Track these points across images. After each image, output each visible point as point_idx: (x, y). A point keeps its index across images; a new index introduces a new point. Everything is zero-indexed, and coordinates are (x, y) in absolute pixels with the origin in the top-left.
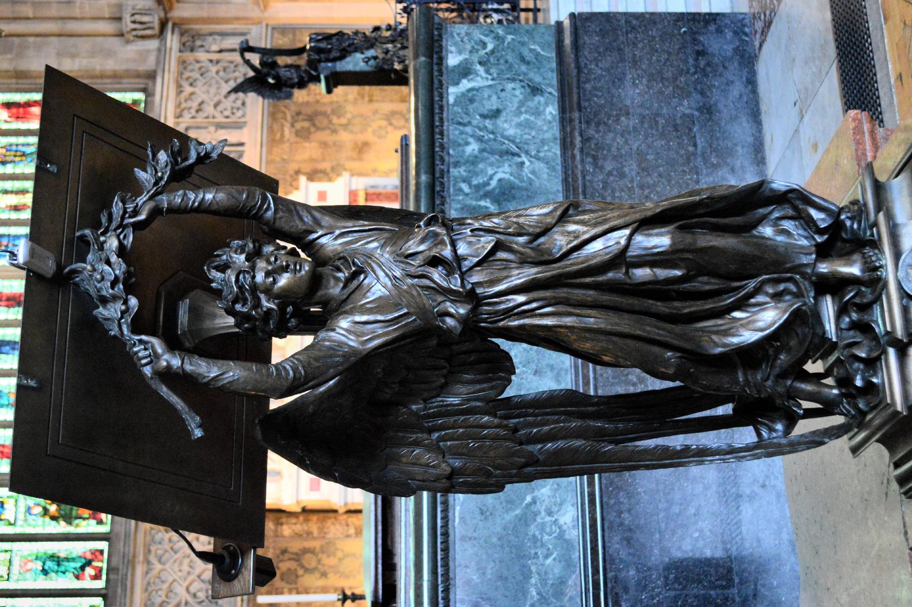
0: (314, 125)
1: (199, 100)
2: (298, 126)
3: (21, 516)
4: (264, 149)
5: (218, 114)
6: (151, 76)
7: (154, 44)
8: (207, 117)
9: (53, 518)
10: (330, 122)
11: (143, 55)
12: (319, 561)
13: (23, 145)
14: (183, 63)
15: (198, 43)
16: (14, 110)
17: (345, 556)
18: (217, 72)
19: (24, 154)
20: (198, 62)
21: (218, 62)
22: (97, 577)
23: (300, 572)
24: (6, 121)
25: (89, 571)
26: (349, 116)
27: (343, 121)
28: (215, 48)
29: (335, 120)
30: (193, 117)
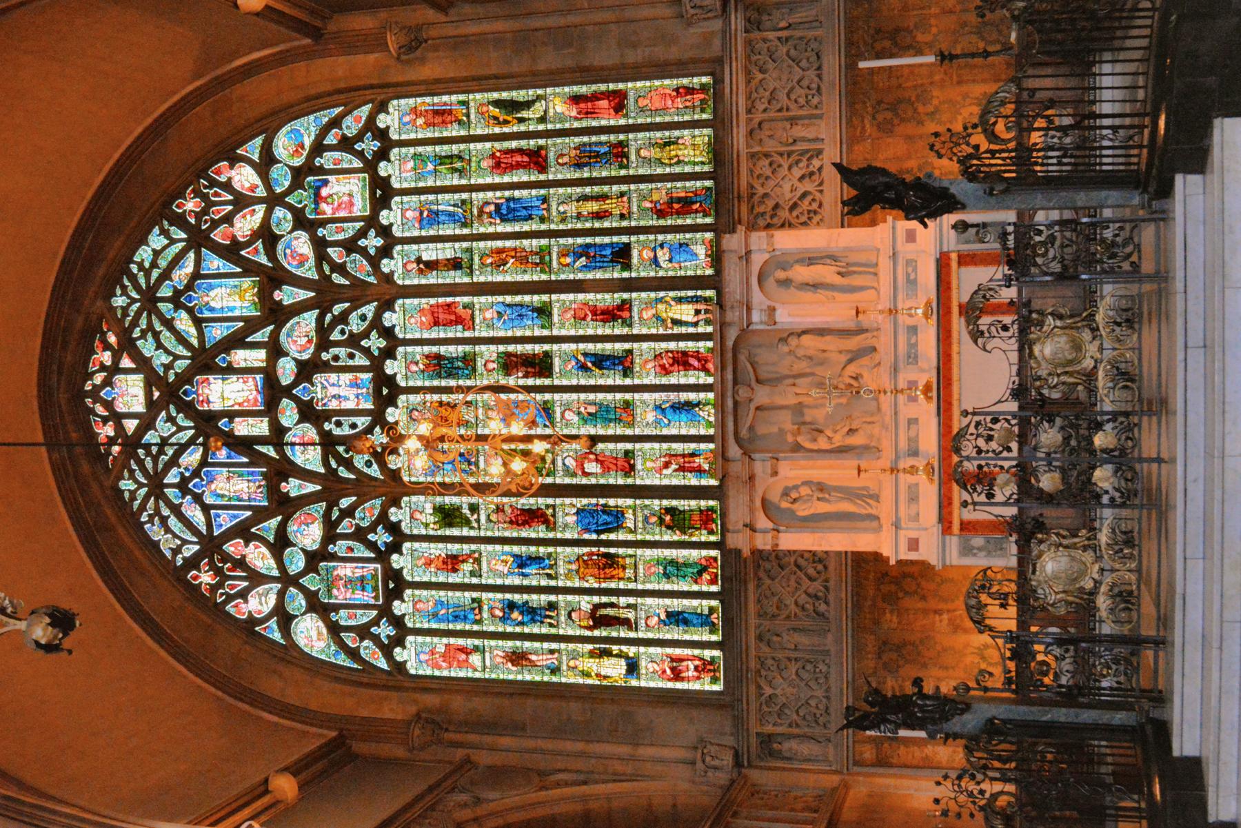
0: (897, 115)
1: (772, 88)
2: (880, 117)
3: (640, 525)
4: (844, 146)
5: (793, 106)
6: (719, 61)
7: (717, 25)
8: (780, 110)
9: (668, 527)
10: (915, 110)
11: (707, 38)
12: (918, 585)
13: (596, 144)
14: (749, 43)
15: (765, 17)
16: (582, 105)
17: (945, 650)
18: (788, 54)
19: (598, 155)
20: (765, 40)
21: (787, 39)
22: (713, 582)
23: (901, 595)
24: (576, 119)
25: (706, 576)
26: (935, 102)
27: (930, 109)
28: (783, 24)
29: (921, 109)
30: (765, 110)
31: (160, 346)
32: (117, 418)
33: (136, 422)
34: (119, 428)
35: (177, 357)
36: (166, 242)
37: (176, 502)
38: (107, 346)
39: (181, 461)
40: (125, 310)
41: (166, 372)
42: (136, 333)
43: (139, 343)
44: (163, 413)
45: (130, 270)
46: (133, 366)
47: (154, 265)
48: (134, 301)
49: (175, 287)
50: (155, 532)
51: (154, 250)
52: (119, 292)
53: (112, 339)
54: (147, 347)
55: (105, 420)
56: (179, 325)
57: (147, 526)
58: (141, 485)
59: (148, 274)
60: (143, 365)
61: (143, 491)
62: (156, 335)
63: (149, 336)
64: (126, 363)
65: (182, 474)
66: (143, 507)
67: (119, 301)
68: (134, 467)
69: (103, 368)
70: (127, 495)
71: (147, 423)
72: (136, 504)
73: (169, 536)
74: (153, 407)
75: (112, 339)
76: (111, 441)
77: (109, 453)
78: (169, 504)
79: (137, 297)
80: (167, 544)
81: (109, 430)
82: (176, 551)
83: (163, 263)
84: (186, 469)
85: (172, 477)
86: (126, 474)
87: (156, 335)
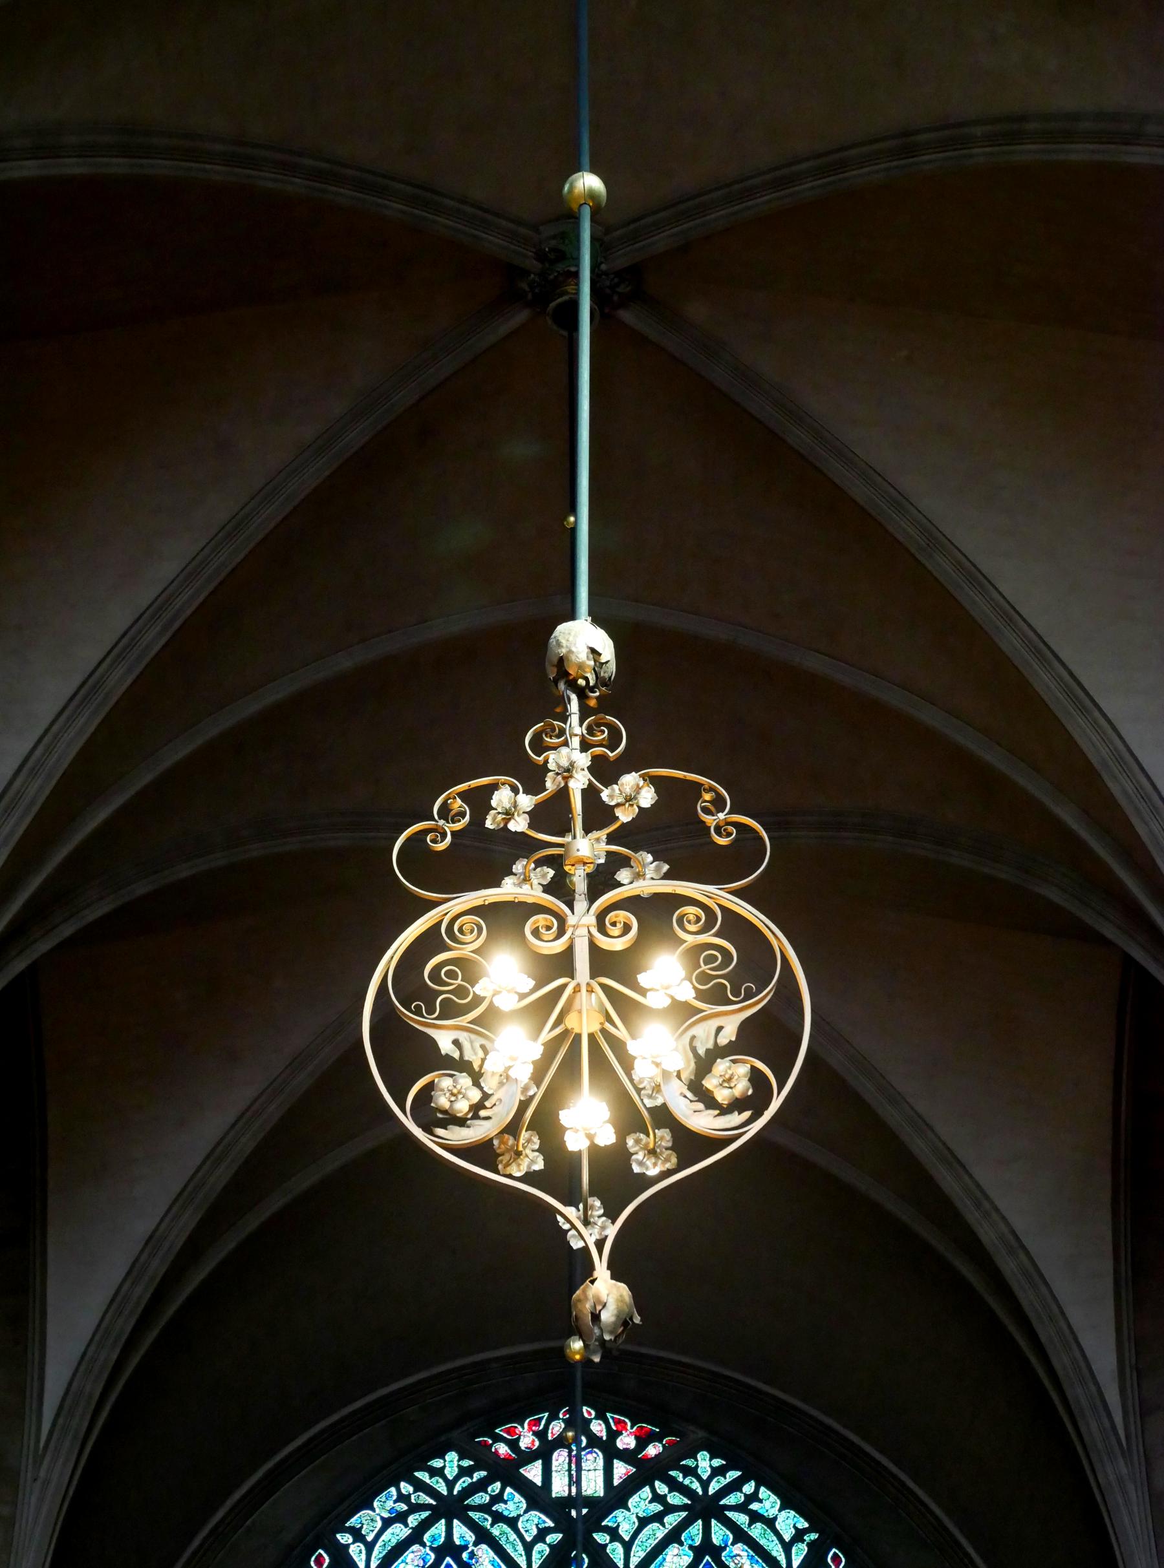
31: (644, 1522)
32: (544, 1453)
33: (538, 1481)
34: (529, 1457)
35: (628, 1546)
36: (787, 1537)
37: (427, 1537)
38: (642, 1442)
39: (484, 1546)
40: (691, 1472)
41: (607, 1530)
42: (662, 1488)
43: (646, 1492)
44: (550, 1524)
45: (748, 1481)
46: (616, 1482)
47: (755, 1517)
48: (705, 1484)
49: (724, 1549)
50: (386, 1503)
51: (775, 1518)
52: (717, 1462)
53: (653, 1450)
54: (641, 1502)
55: (541, 1435)
56: (673, 1549)
57: (393, 1490)
58: (450, 1484)
59: (741, 1508)
60: (617, 1497)
61: (442, 1489)
62: (658, 1518)
63: (657, 1507)
64: (621, 1470)
65: (465, 1547)
66: (420, 1486)
67: (704, 1463)
68: (477, 1476)
69: (613, 1435)
70: (437, 1463)
71: (537, 1498)
72: (423, 1476)
73: (379, 1524)
74: (557, 1508)
75: (653, 1450)
76: (514, 1445)
77: (498, 1439)
78: (425, 1526)
79: (711, 1491)
80: (367, 1520)
81: (527, 1440)
82: (358, 1535)
83: (757, 1531)
84: (472, 1555)
85: (462, 1533)
86: (466, 1463)
87: (658, 1518)
